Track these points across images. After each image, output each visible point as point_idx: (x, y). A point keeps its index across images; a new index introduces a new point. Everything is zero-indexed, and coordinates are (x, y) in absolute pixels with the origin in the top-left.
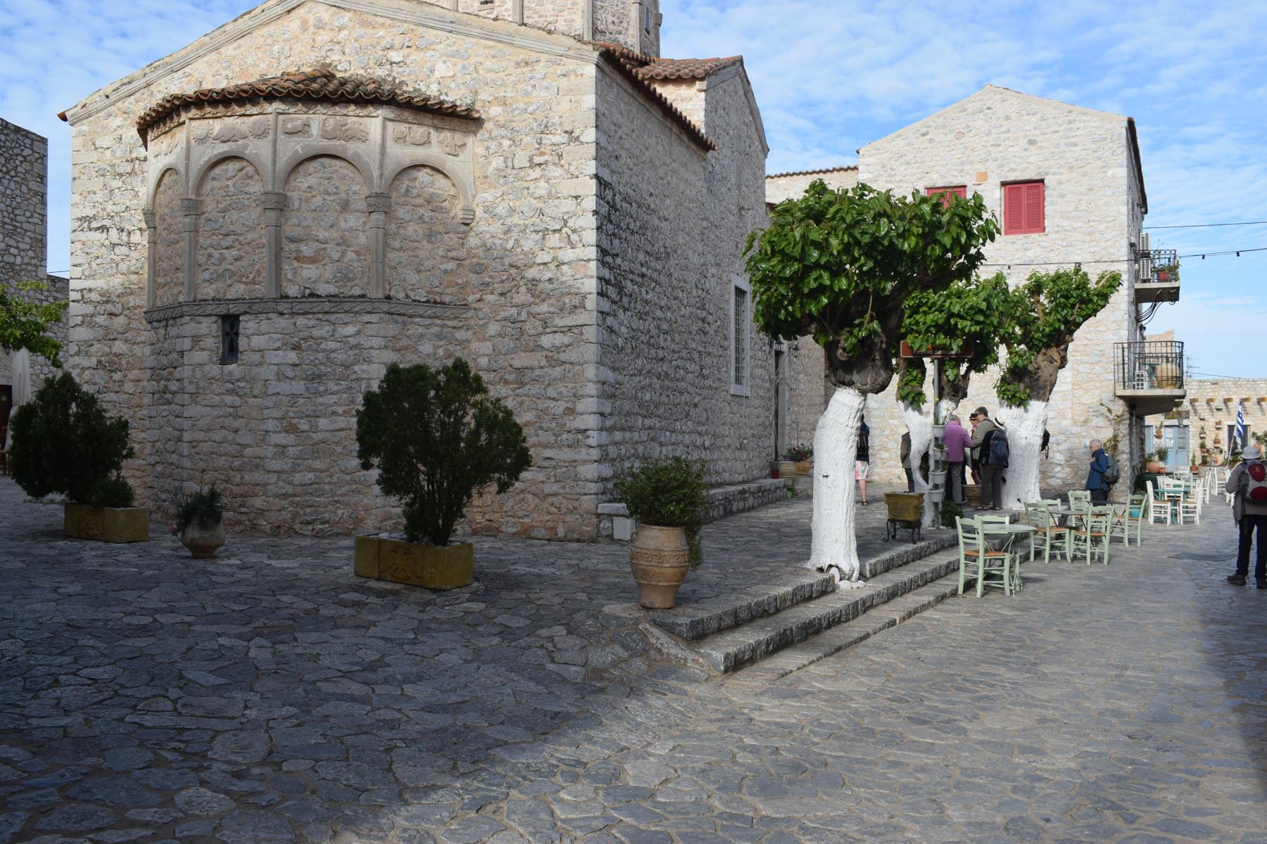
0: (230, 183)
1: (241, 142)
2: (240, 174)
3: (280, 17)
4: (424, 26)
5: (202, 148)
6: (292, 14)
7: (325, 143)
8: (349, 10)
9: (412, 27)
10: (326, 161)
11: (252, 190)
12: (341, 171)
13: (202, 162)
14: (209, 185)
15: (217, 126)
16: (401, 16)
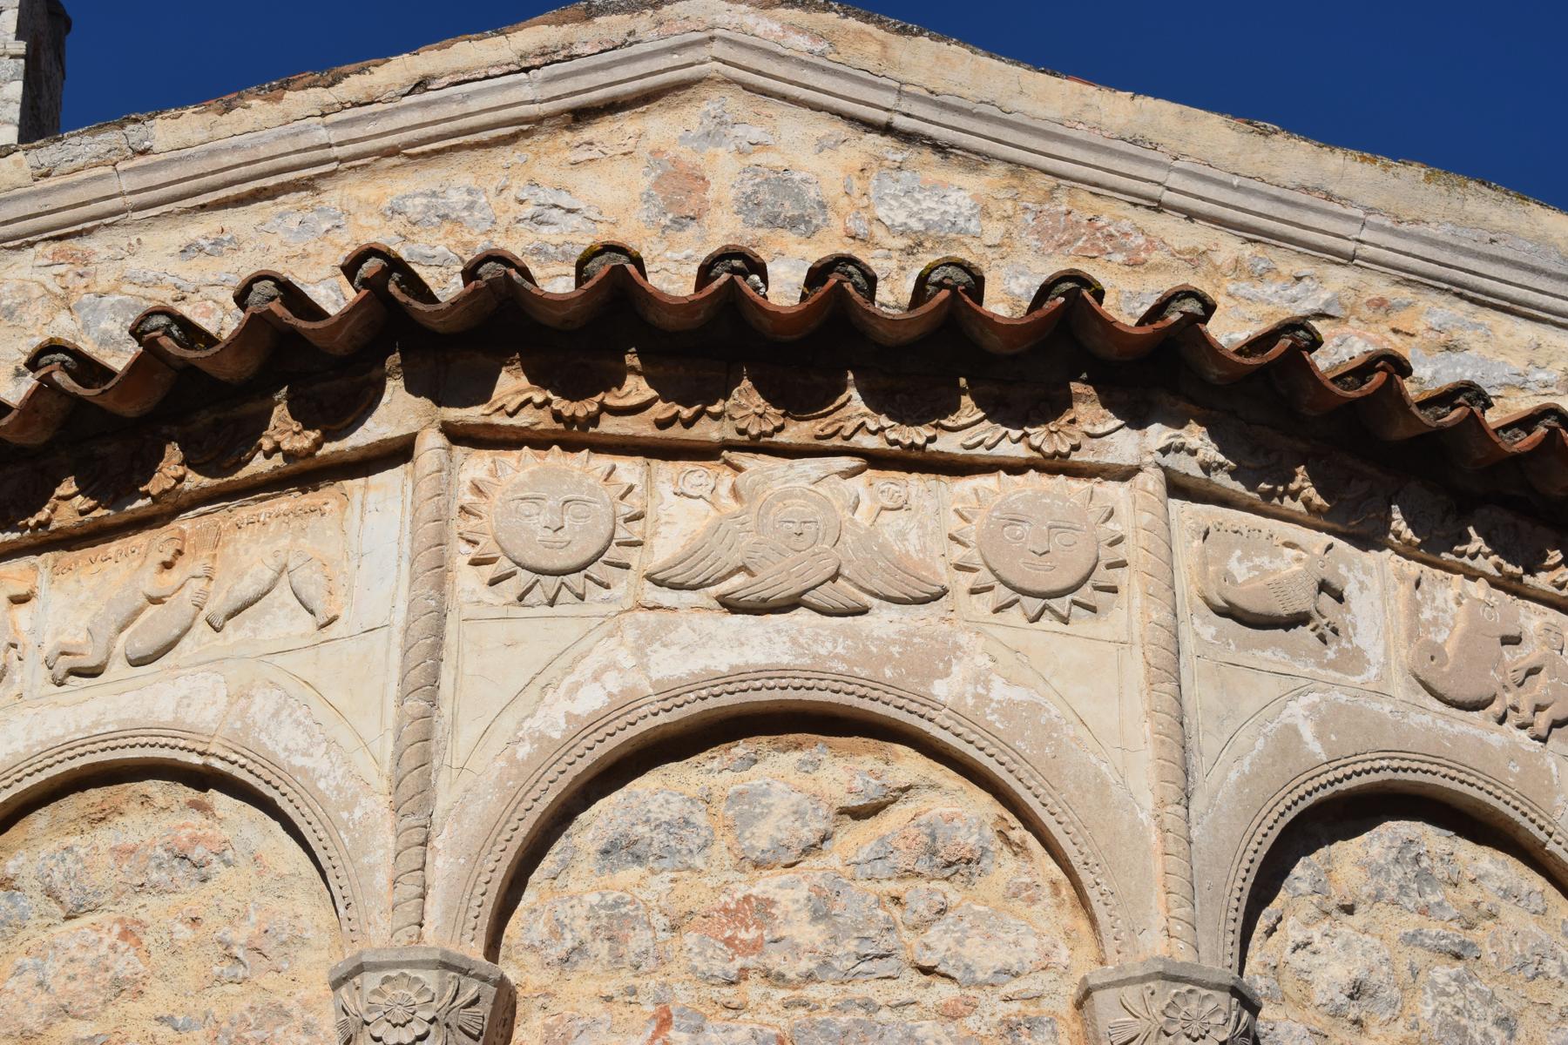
0: (786, 891)
1: (884, 622)
2: (858, 839)
3: (523, 129)
4: (1461, 292)
5: (547, 630)
6: (598, 131)
7: (1433, 719)
8: (978, 160)
9: (1380, 287)
10: (1432, 838)
11: (985, 956)
12: (1512, 916)
13: (554, 717)
14: (571, 885)
15: (683, 508)
16: (1322, 226)
